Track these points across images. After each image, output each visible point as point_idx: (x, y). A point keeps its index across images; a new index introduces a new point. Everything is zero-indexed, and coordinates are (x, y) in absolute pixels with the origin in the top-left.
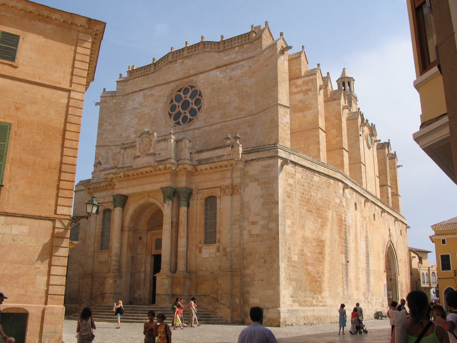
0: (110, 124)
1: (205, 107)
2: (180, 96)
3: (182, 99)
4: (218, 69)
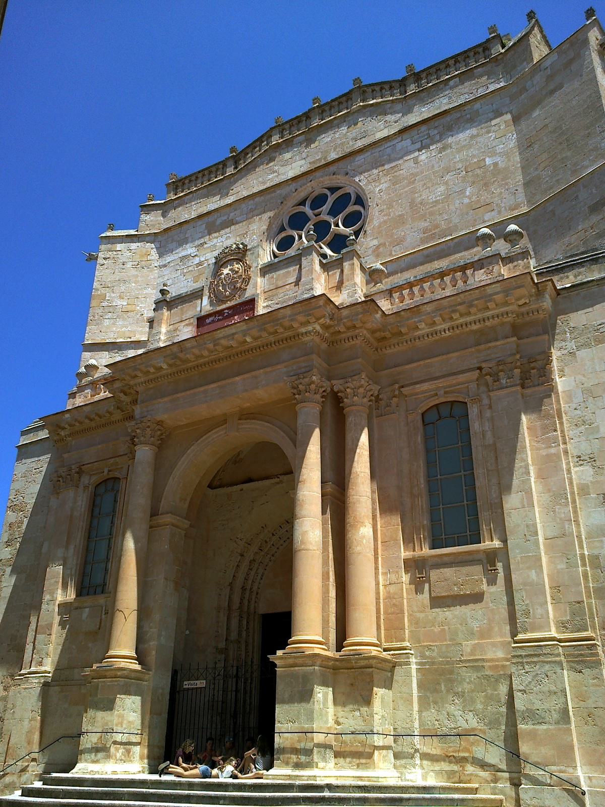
0: (121, 298)
1: (376, 223)
2: (303, 214)
3: (308, 219)
4: (405, 136)
